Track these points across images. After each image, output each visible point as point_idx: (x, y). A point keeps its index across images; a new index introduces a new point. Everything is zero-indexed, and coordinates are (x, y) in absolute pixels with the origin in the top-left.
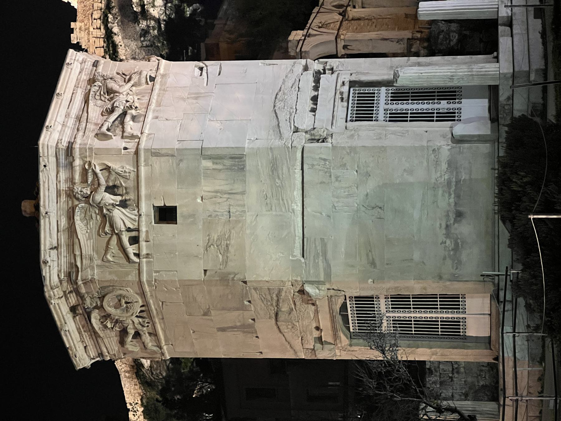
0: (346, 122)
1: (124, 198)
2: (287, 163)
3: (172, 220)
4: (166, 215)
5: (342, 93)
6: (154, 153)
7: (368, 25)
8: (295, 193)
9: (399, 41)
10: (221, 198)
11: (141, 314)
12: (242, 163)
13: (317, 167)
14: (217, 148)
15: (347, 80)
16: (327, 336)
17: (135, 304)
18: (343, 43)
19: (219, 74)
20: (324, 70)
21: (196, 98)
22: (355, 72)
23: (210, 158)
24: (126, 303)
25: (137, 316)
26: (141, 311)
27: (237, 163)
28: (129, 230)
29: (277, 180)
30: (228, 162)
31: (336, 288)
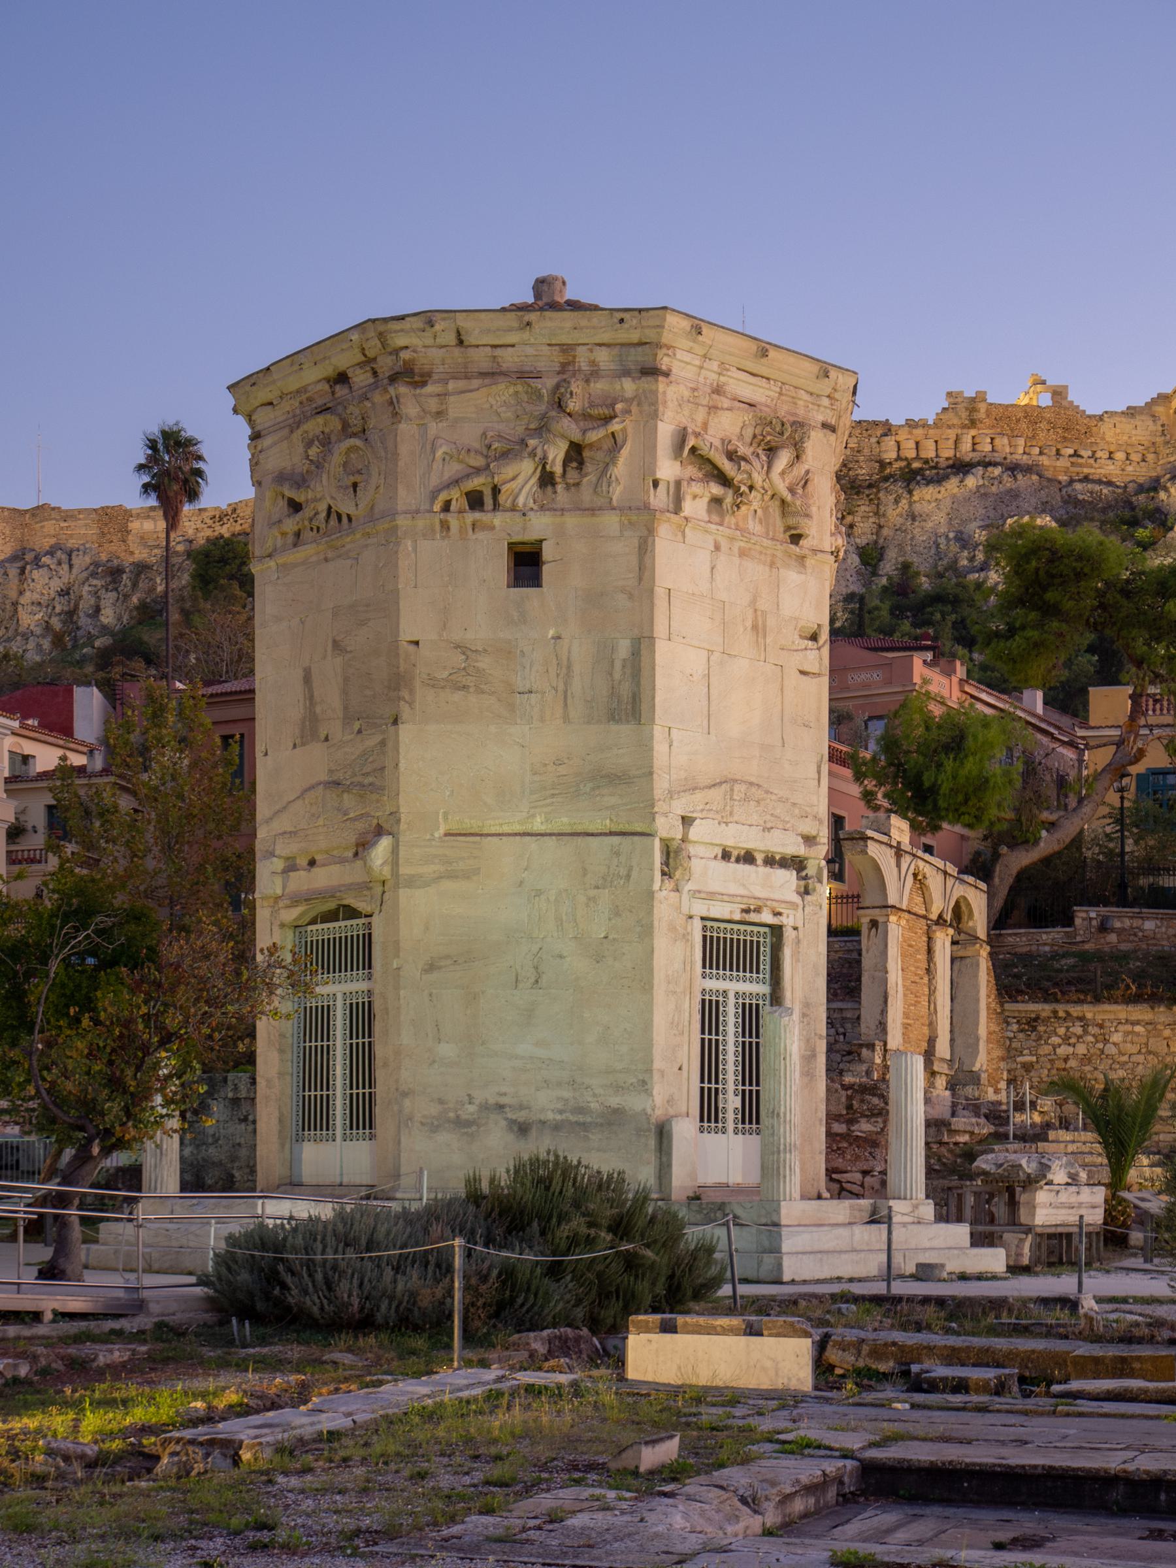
0: (702, 918)
2: (625, 804)
3: (516, 578)
5: (758, 910)
6: (646, 542)
7: (918, 967)
8: (565, 820)
9: (882, 1026)
10: (558, 675)
11: (334, 516)
12: (623, 717)
13: (615, 861)
14: (654, 669)
15: (784, 920)
18: (881, 920)
19: (802, 673)
20: (806, 878)
21: (755, 627)
22: (801, 936)
23: (636, 653)
25: (330, 508)
27: (624, 707)
29: (590, 785)
30: (625, 690)
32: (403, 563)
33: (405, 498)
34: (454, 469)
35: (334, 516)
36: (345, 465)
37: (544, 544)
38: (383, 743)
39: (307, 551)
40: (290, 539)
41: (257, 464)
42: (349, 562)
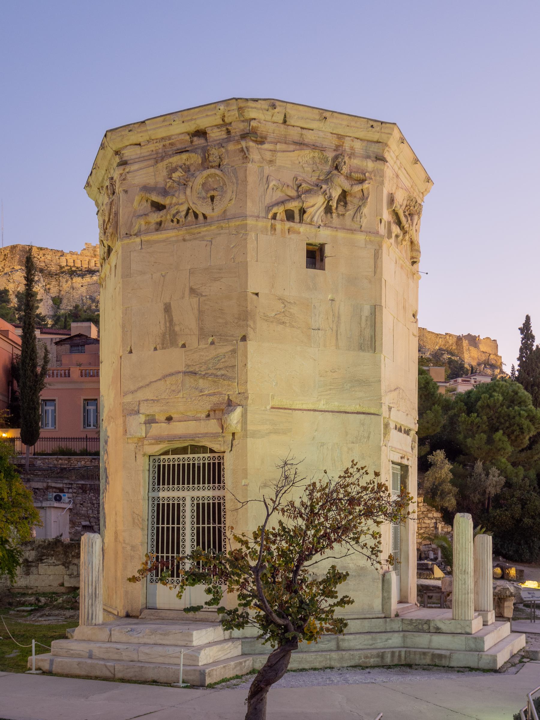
1: (334, 211)
4: (315, 256)
6: (378, 252)
16: (156, 429)
17: (211, 208)
24: (212, 198)
25: (189, 209)
26: (196, 216)
28: (303, 212)
31: (235, 442)
32: (251, 246)
33: (253, 207)
34: (278, 195)
35: (191, 215)
36: (204, 185)
37: (326, 246)
38: (234, 351)
39: (170, 234)
40: (153, 227)
41: (124, 180)
42: (205, 243)
